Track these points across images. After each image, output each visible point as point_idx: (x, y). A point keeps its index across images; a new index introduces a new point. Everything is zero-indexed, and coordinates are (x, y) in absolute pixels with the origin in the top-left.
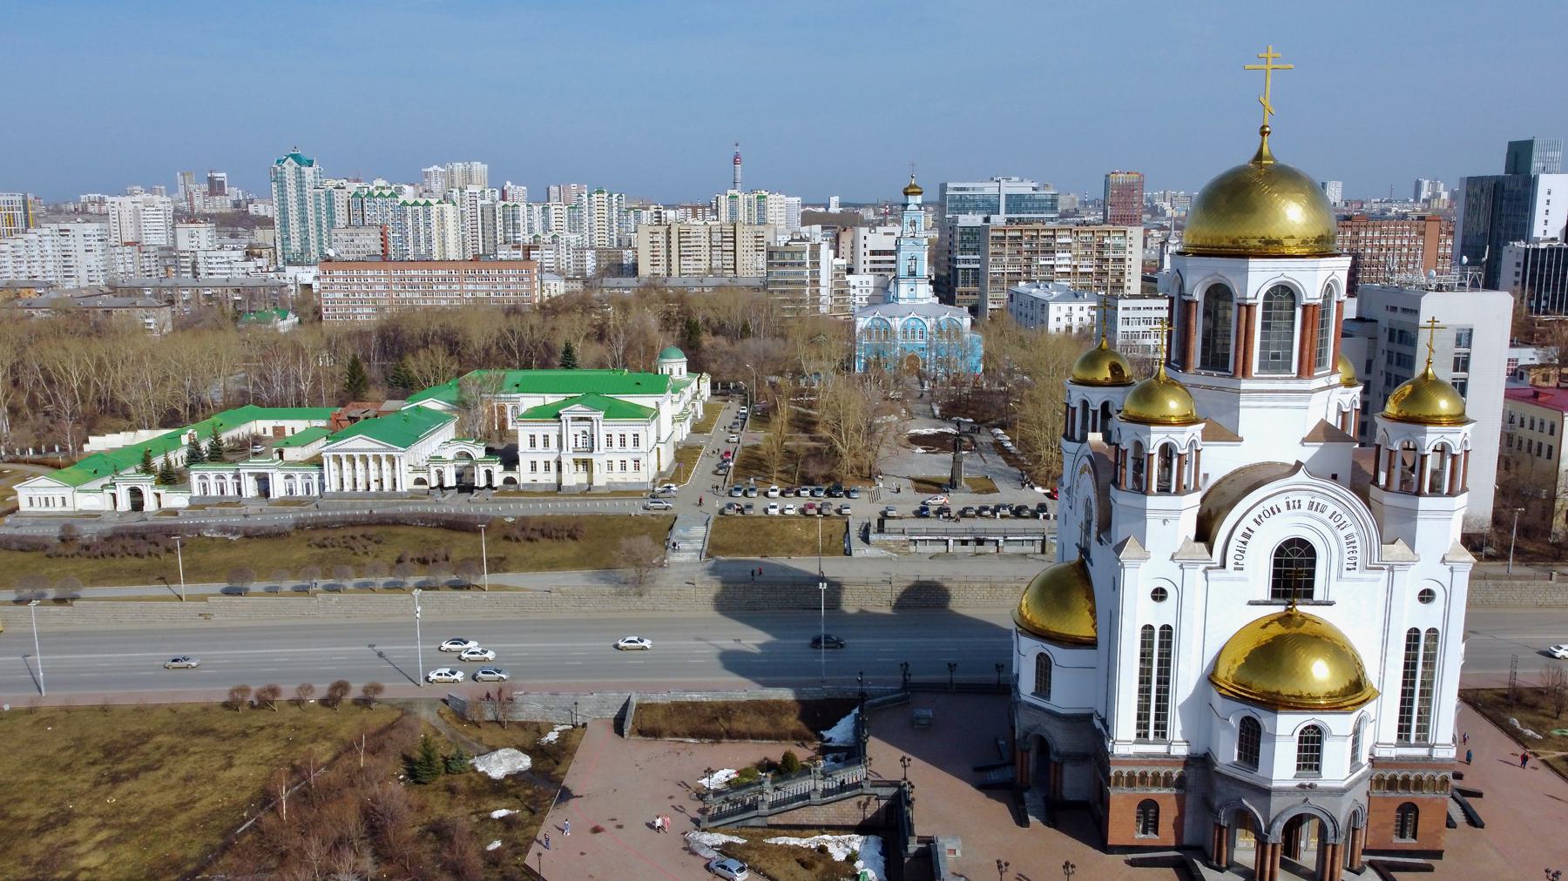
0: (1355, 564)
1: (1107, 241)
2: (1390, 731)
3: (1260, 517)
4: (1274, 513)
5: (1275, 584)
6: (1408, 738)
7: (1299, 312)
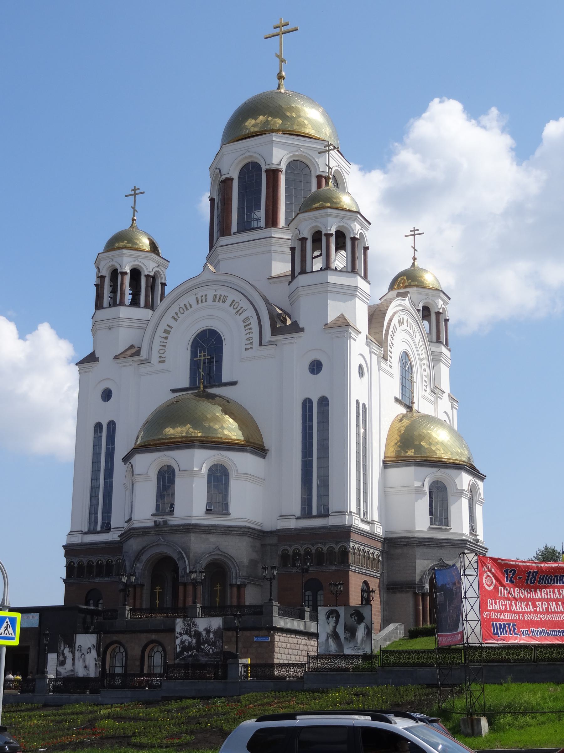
0: (251, 344)
3: (177, 314)
4: (187, 309)
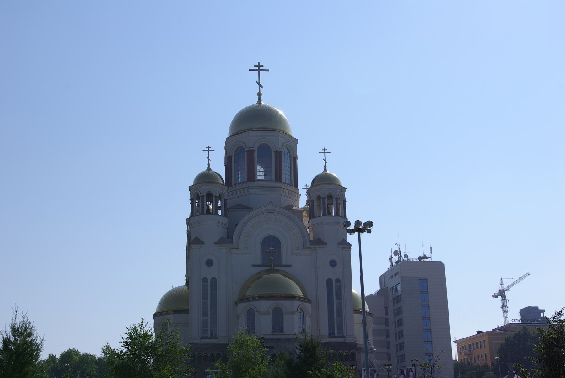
6: (334, 333)
7: (273, 154)
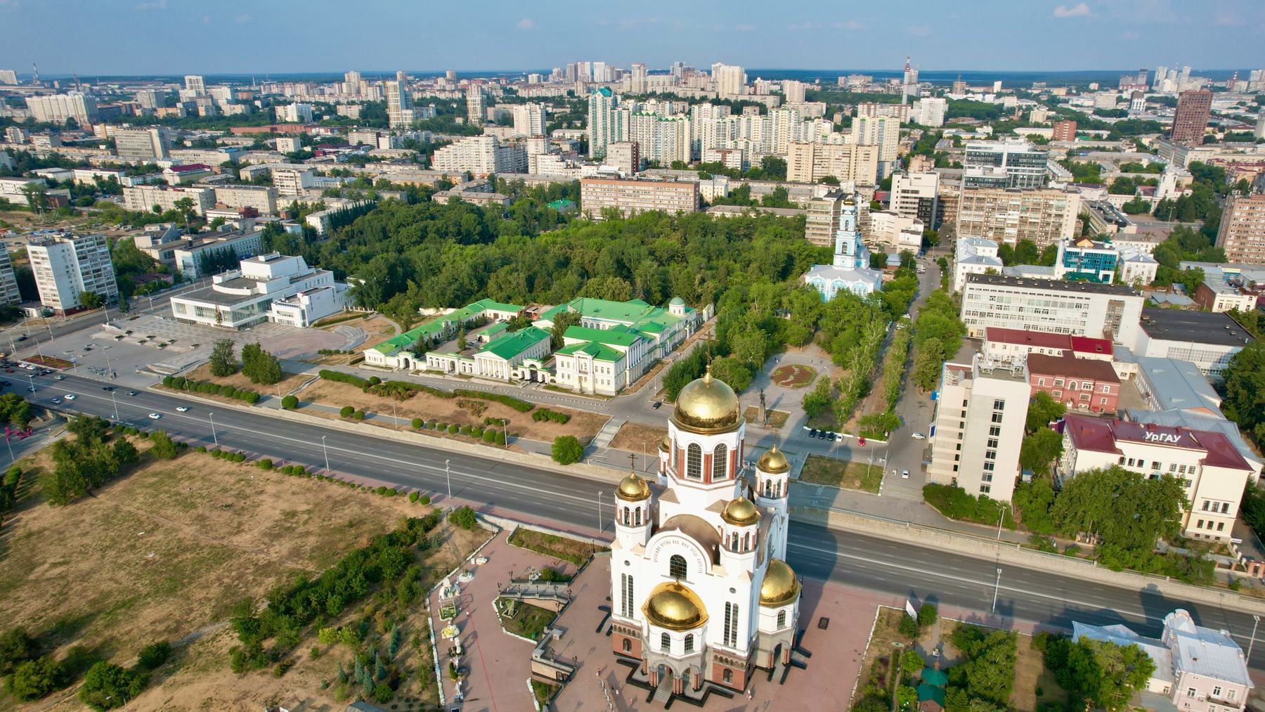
1: (1051, 202)
2: (722, 641)
5: (671, 570)
